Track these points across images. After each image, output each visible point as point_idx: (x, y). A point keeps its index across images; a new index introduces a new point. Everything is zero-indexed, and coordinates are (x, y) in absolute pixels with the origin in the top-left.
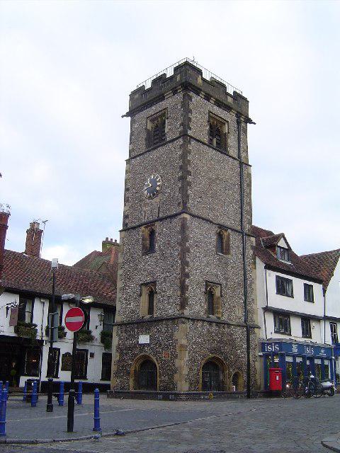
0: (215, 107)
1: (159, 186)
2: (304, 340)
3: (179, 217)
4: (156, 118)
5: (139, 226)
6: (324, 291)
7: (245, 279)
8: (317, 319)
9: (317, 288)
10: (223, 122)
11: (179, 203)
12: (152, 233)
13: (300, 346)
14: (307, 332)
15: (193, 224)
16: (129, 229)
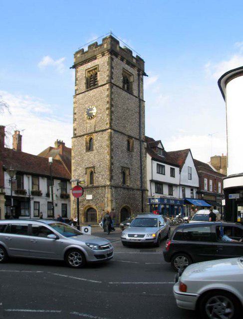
0: (126, 66)
2: (170, 196)
3: (107, 131)
4: (91, 71)
5: (83, 135)
6: (180, 171)
7: (141, 166)
8: (176, 186)
9: (177, 170)
10: (131, 75)
11: (107, 123)
12: (91, 139)
13: (168, 200)
14: (171, 193)
16: (77, 137)
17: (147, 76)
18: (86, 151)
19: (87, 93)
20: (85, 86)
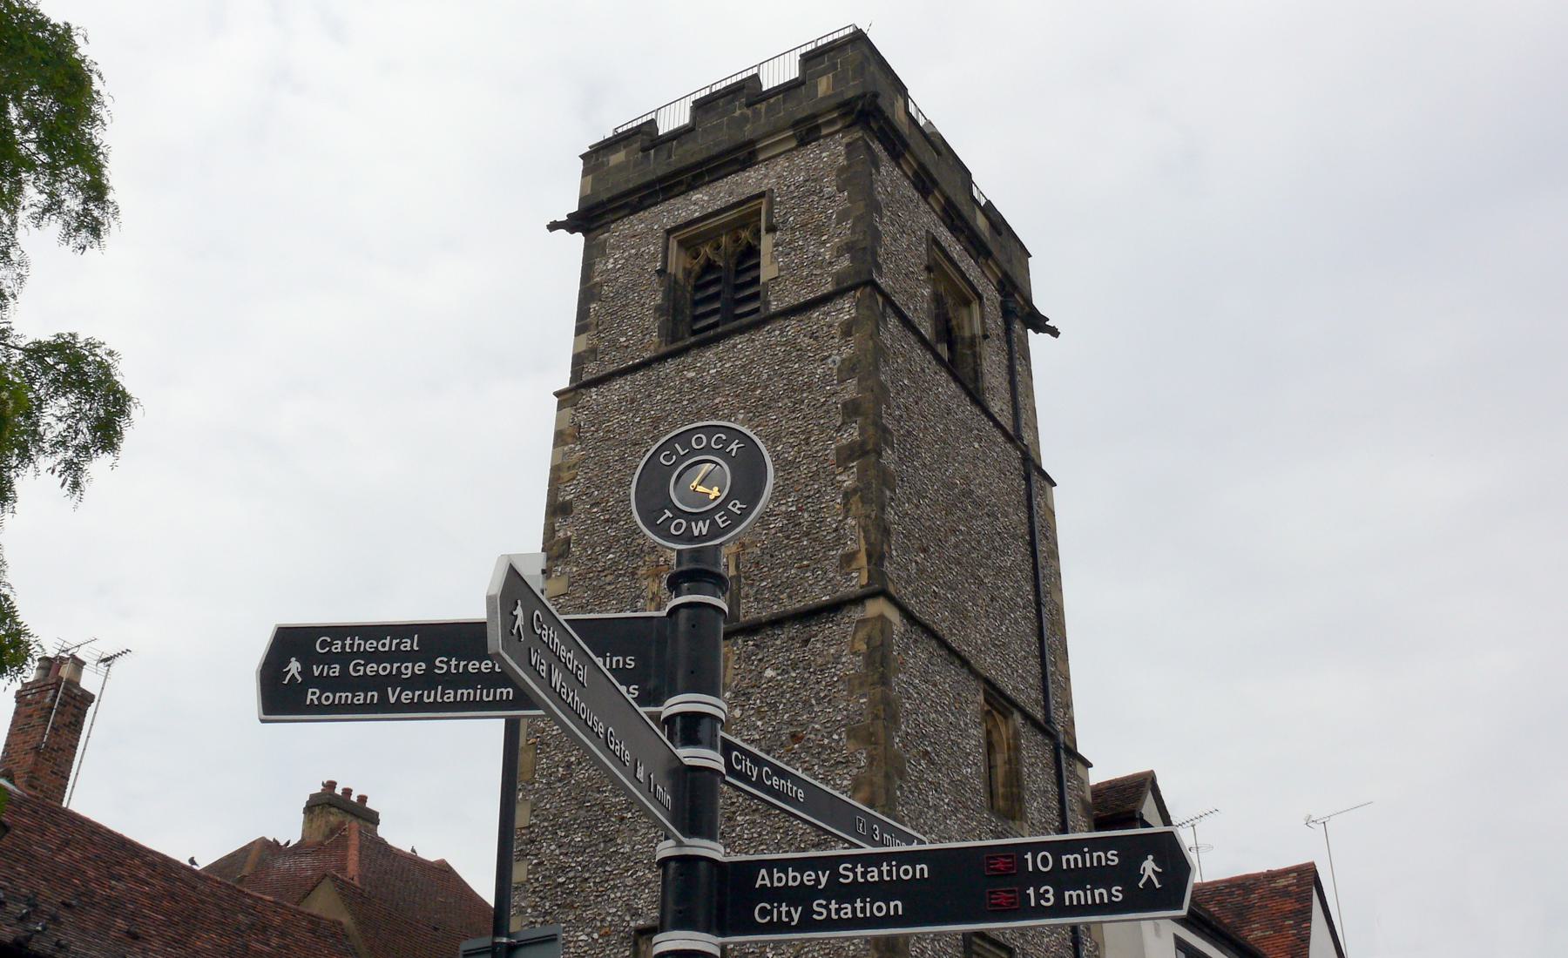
3: (857, 614)
11: (849, 558)
19: (670, 366)
20: (652, 323)
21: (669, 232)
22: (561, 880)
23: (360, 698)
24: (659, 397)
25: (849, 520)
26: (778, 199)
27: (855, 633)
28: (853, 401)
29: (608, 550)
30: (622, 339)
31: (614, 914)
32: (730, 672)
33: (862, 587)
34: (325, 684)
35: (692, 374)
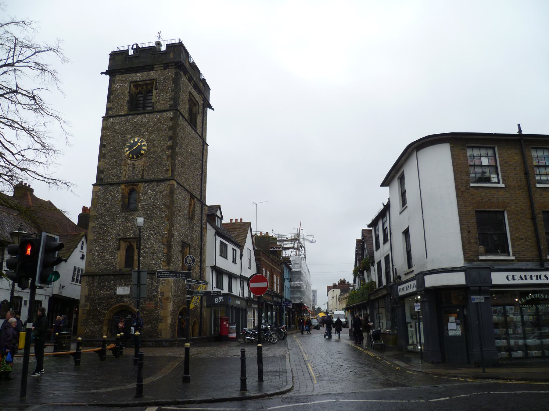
0: (193, 90)
1: (144, 150)
3: (168, 182)
4: (142, 86)
11: (167, 170)
15: (178, 190)
16: (104, 185)
17: (213, 109)
18: (122, 211)
19: (130, 117)
21: (131, 82)
22: (103, 227)
23: (165, 277)
24: (127, 124)
25: (168, 162)
26: (158, 82)
27: (167, 187)
28: (171, 136)
29: (114, 157)
30: (119, 107)
31: (115, 235)
32: (141, 190)
33: (170, 177)
34: (162, 276)
35: (135, 121)
